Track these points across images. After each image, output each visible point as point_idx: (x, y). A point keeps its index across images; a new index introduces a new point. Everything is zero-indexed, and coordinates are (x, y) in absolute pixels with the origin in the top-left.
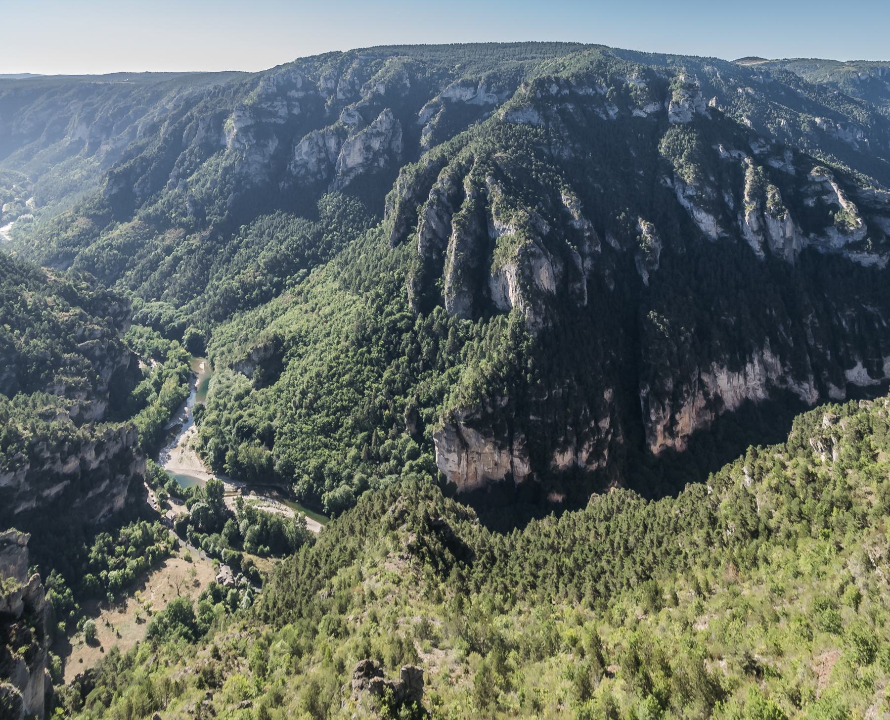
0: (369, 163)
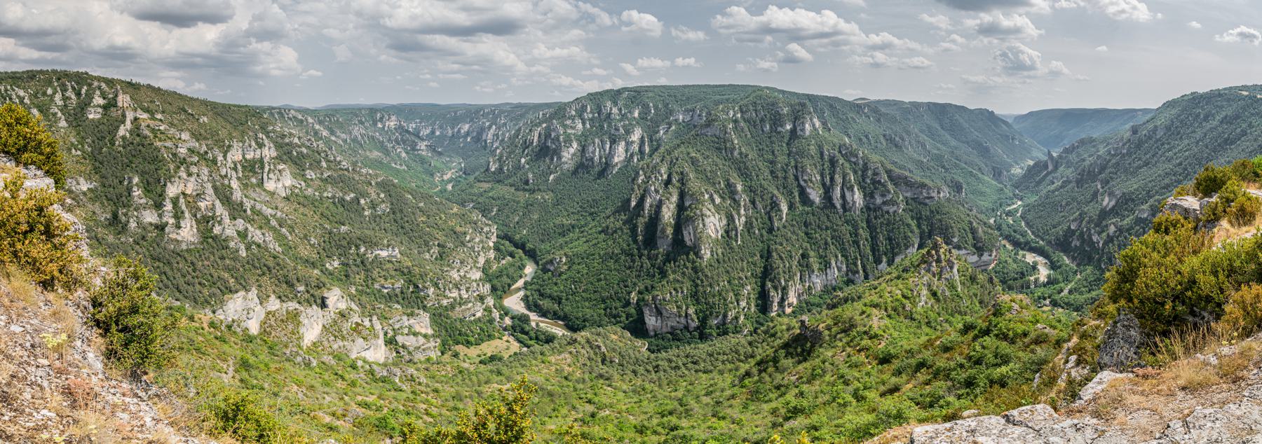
0: (629, 159)
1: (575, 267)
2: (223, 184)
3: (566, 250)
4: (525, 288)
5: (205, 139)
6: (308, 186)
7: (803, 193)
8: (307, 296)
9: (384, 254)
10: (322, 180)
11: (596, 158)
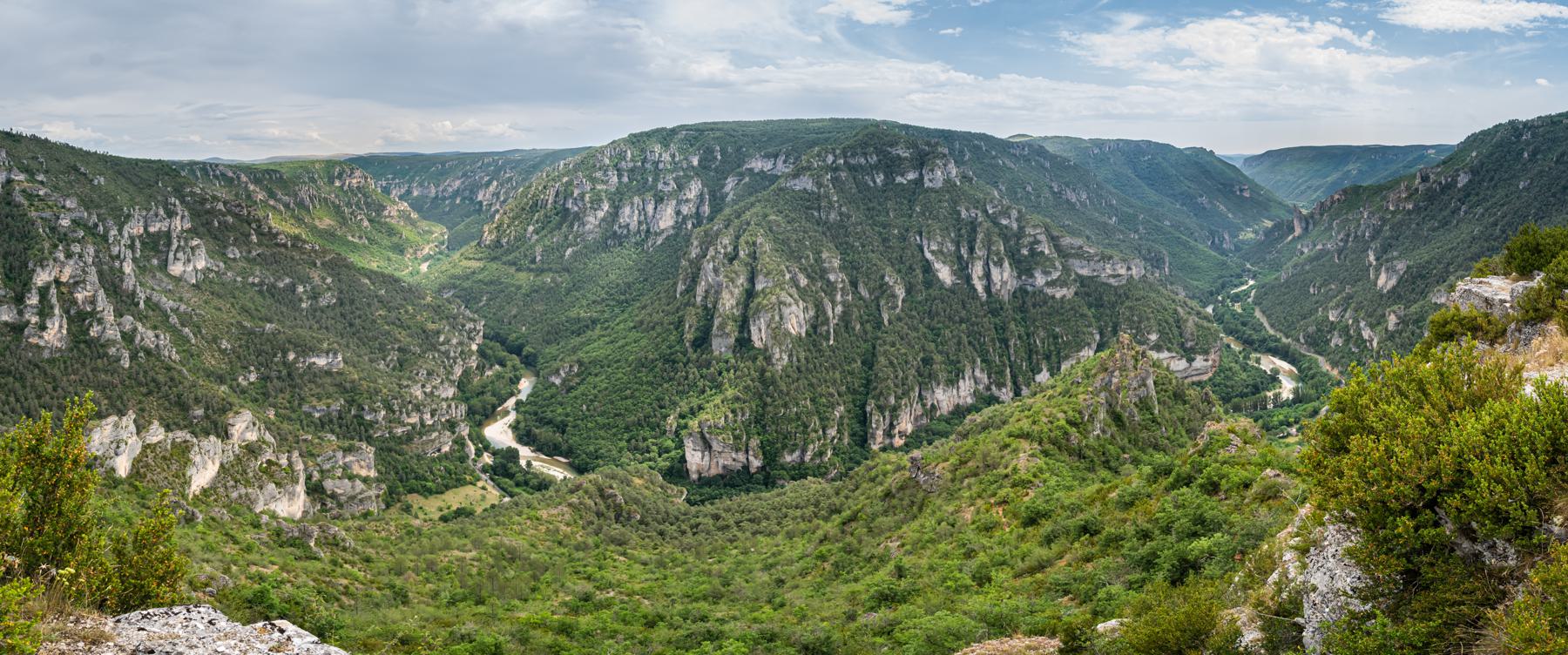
0: (678, 226)
1: (591, 379)
2: (112, 268)
3: (581, 354)
4: (517, 409)
5: (98, 206)
6: (229, 268)
7: (928, 268)
8: (205, 424)
9: (321, 362)
10: (248, 260)
11: (634, 226)
